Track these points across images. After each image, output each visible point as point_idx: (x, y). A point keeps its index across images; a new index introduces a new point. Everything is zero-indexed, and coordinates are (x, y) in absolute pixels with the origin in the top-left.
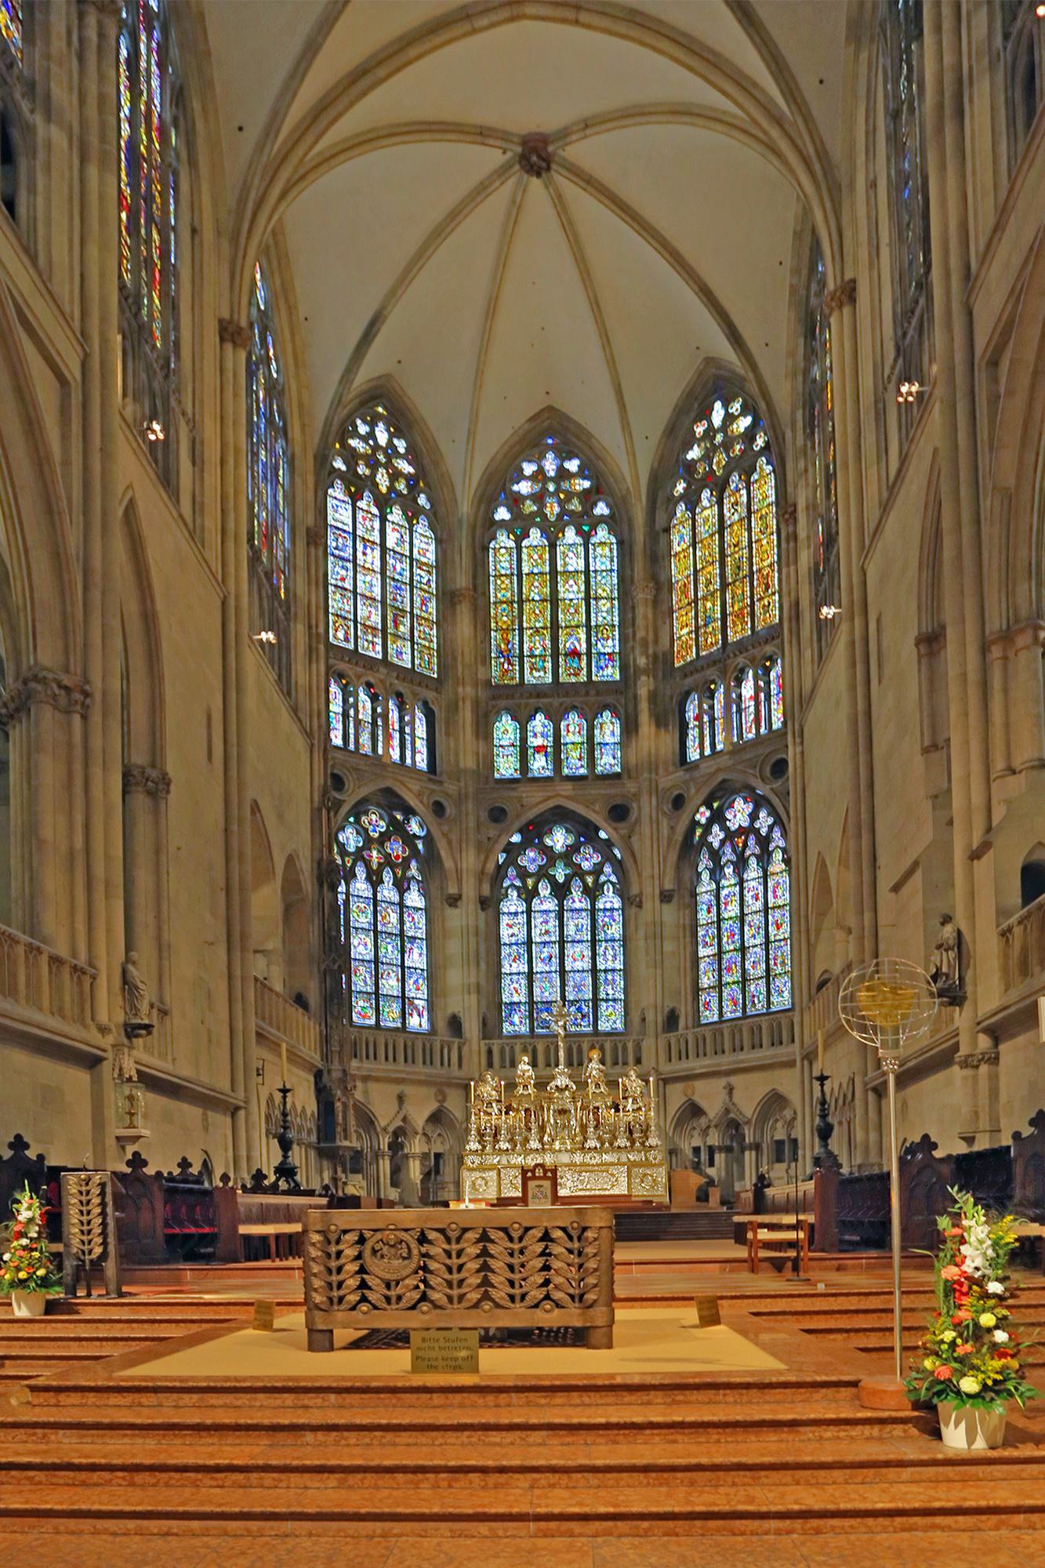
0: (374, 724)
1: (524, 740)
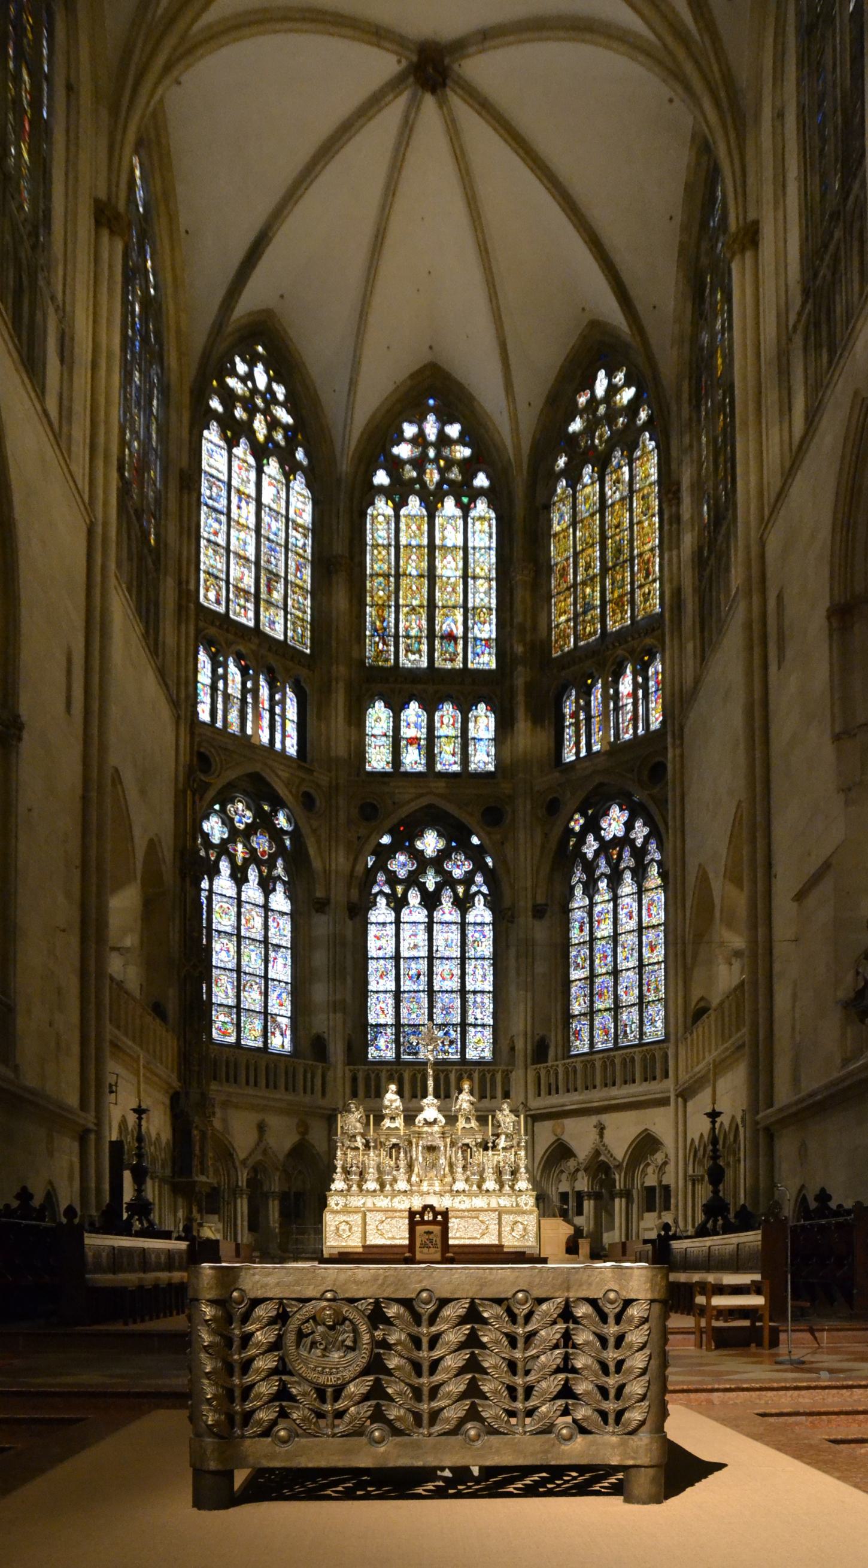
1: (397, 728)
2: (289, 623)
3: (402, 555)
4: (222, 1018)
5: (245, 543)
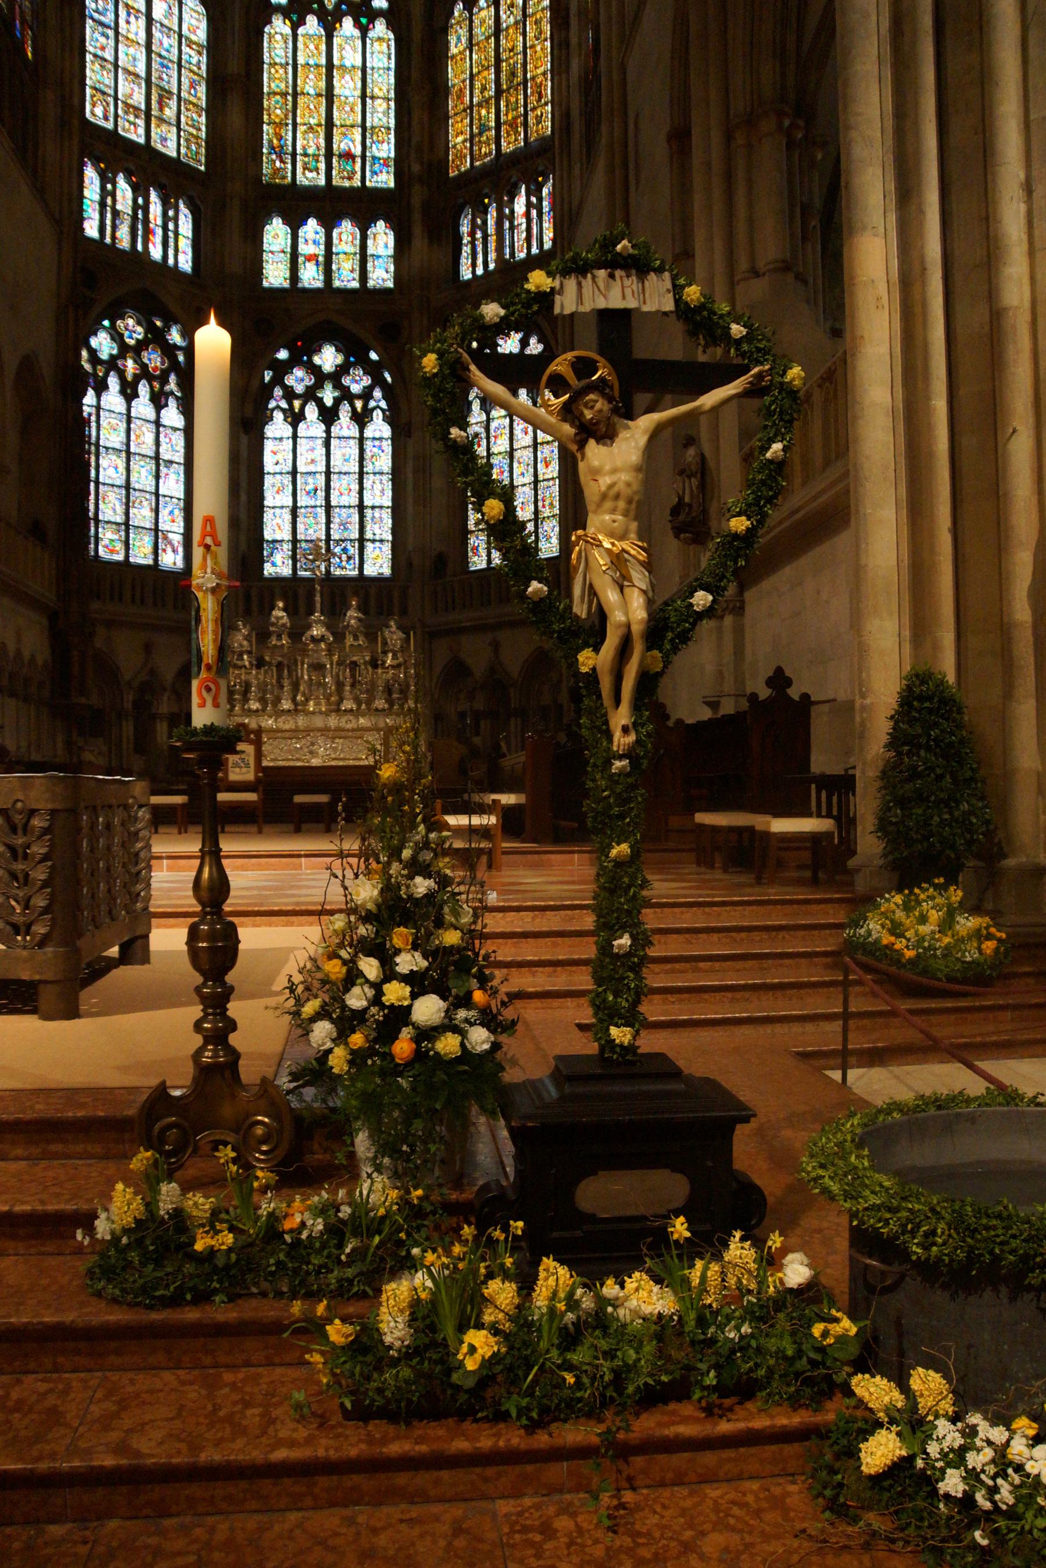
0: (134, 218)
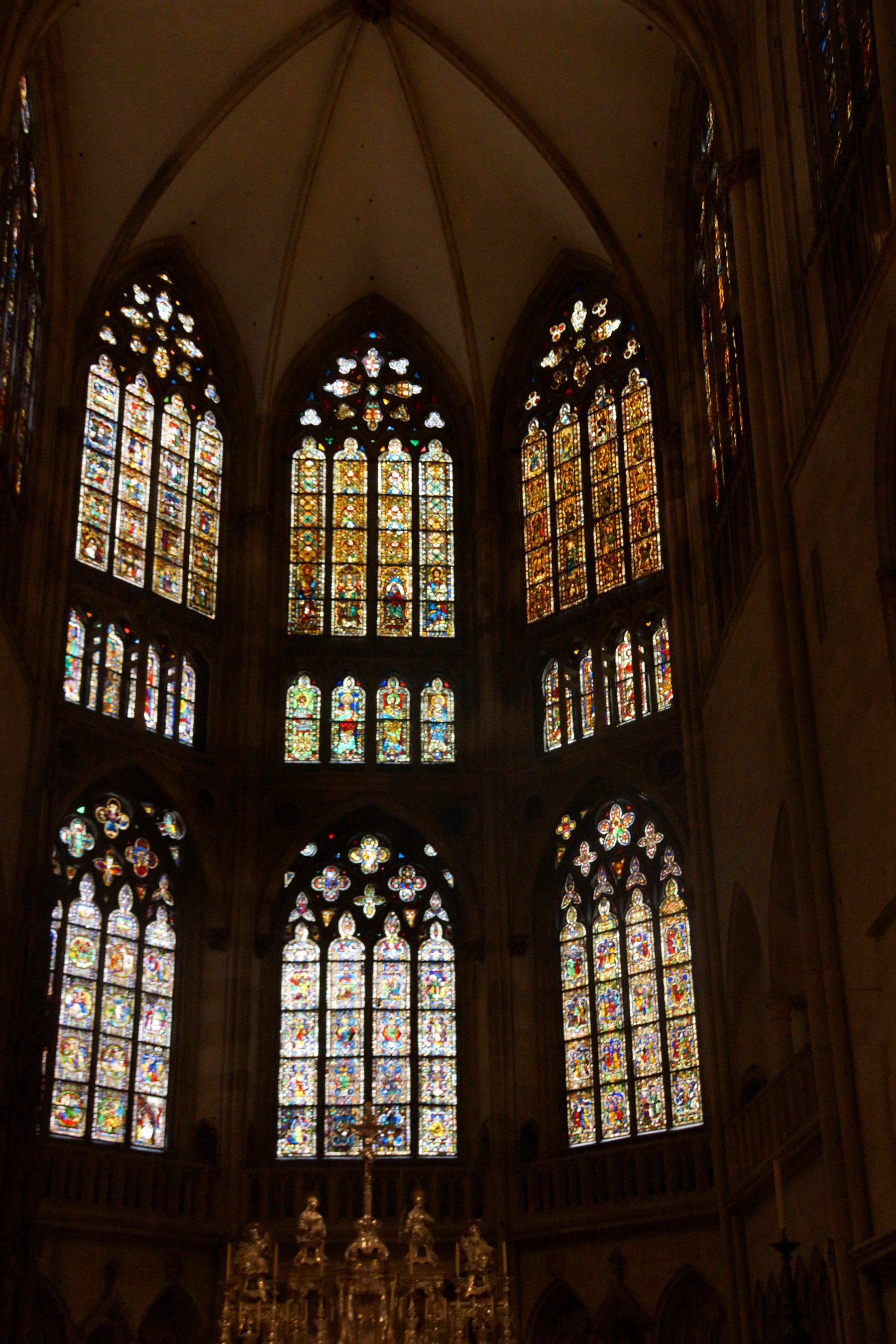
0: (125, 676)
2: (189, 584)
3: (335, 506)
4: (66, 1101)
5: (137, 492)
